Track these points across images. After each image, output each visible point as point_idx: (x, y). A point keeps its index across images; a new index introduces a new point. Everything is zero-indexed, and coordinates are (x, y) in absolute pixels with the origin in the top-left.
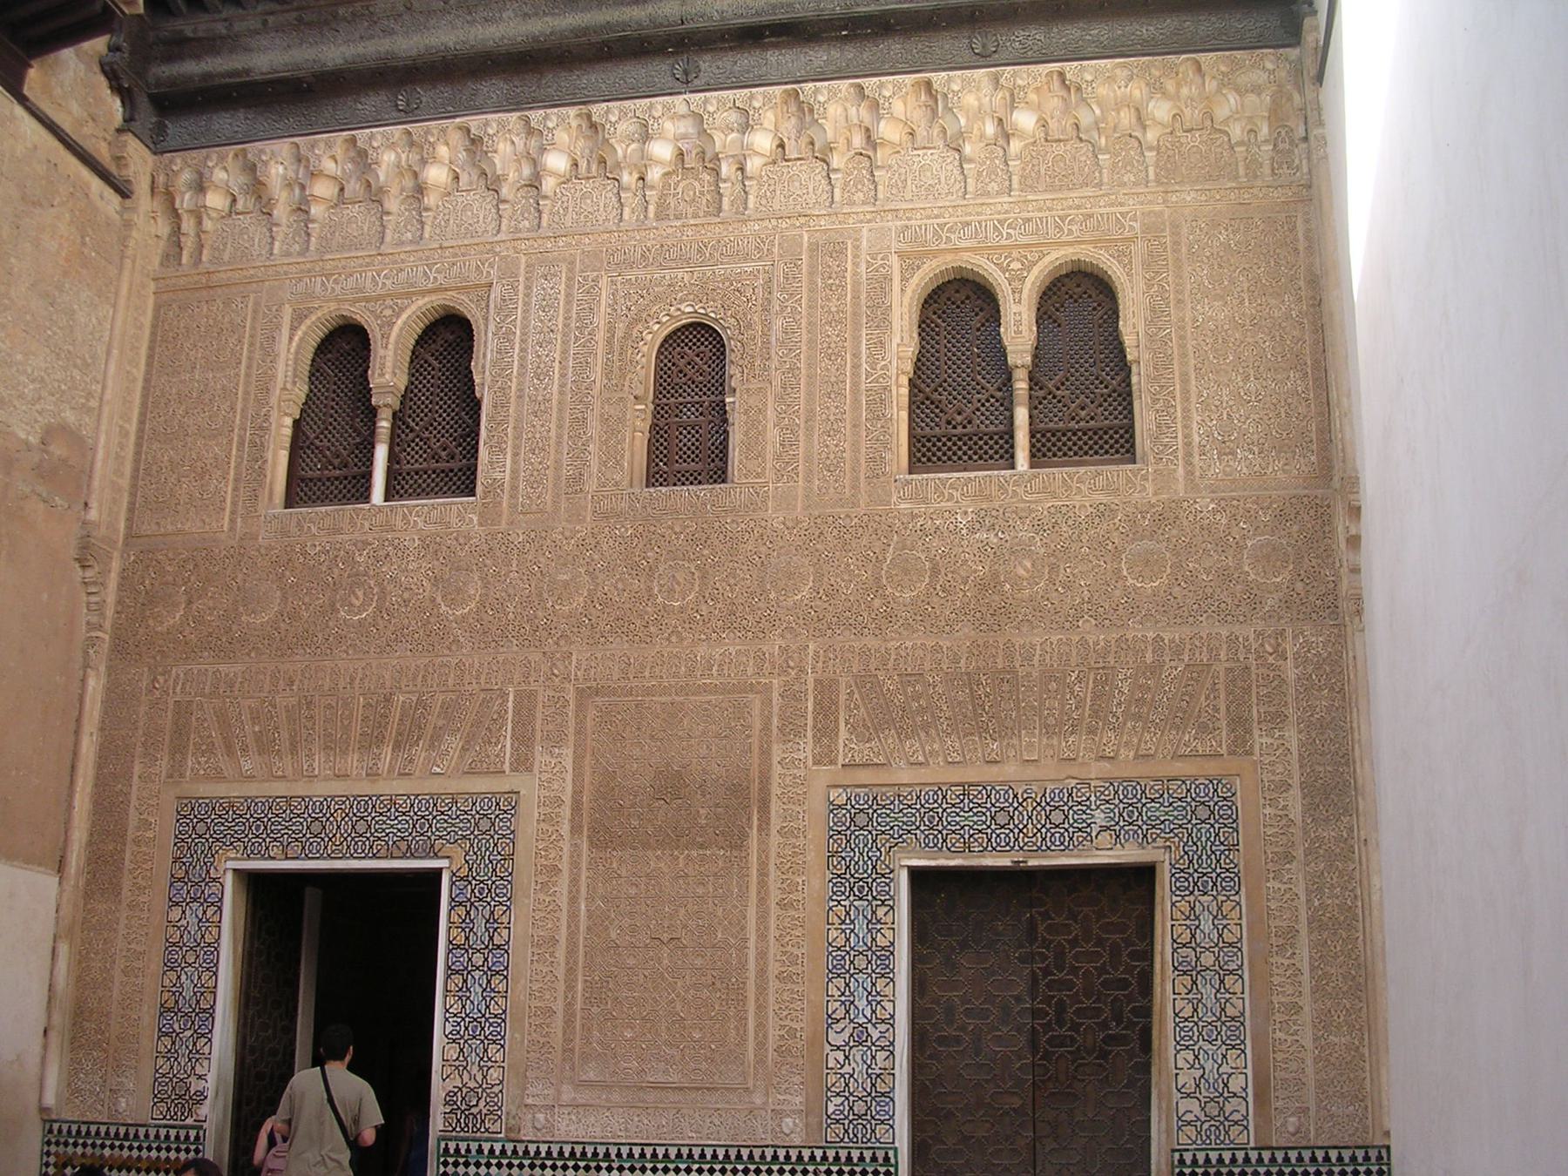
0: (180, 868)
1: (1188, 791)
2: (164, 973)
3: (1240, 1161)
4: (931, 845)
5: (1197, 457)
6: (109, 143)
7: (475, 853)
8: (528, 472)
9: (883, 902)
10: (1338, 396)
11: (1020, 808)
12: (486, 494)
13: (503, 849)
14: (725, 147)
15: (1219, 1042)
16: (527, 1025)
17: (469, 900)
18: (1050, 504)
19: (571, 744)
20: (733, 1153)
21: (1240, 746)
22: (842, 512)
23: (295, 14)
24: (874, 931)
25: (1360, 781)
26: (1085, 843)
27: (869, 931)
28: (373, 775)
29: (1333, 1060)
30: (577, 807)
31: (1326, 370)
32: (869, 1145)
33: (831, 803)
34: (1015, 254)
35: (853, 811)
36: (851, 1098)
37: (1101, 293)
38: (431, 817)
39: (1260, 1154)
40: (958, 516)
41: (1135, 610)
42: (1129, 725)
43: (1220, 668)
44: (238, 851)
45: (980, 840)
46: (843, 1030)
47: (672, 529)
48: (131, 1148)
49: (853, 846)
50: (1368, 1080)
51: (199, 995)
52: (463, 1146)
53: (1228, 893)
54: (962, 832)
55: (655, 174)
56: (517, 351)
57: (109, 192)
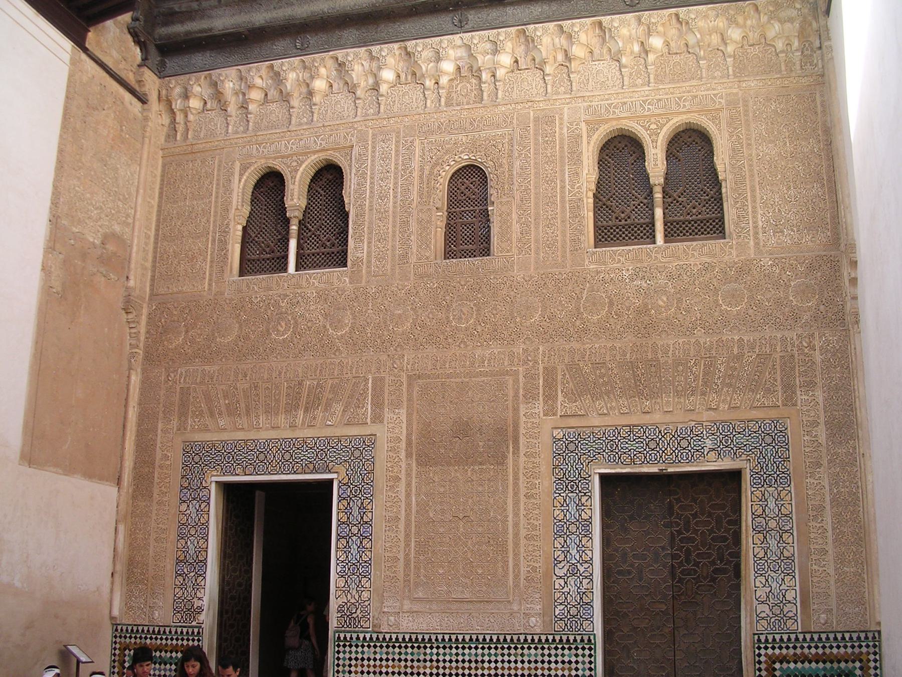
0: (186, 481)
1: (760, 427)
2: (178, 540)
3: (793, 640)
4: (612, 460)
5: (761, 235)
6: (134, 73)
7: (352, 470)
8: (377, 253)
9: (585, 494)
10: (842, 197)
11: (663, 439)
12: (353, 265)
13: (368, 467)
14: (484, 63)
15: (780, 572)
16: (383, 567)
17: (349, 496)
18: (677, 264)
19: (405, 406)
20: (502, 638)
21: (789, 401)
24: (580, 510)
25: (859, 420)
26: (700, 458)
27: (577, 510)
28: (293, 426)
29: (846, 581)
30: (409, 443)
31: (835, 182)
32: (579, 632)
33: (554, 438)
34: (653, 120)
35: (567, 442)
36: (569, 606)
37: (703, 141)
38: (326, 450)
39: (804, 636)
40: (624, 272)
41: (727, 323)
43: (777, 356)
44: (218, 471)
45: (640, 458)
46: (563, 567)
47: (459, 283)
48: (161, 639)
49: (567, 462)
50: (867, 592)
51: (198, 553)
52: (348, 636)
53: (784, 486)
54: (629, 453)
55: (444, 80)
56: (368, 184)
57: (135, 101)
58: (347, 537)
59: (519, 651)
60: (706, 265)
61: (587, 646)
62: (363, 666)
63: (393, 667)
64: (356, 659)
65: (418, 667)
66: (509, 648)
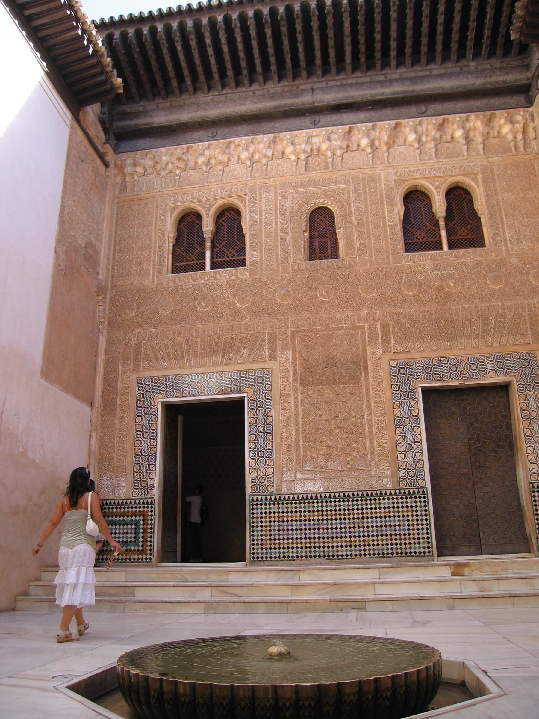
12: (251, 265)
20: (365, 493)
22: (384, 266)
23: (169, 104)
27: (409, 410)
30: (295, 373)
42: (496, 334)
43: (526, 314)
48: (124, 508)
52: (259, 498)
57: (102, 164)
58: (256, 434)
59: (377, 501)
60: (477, 262)
61: (422, 496)
62: (270, 517)
63: (292, 517)
64: (266, 513)
65: (309, 516)
66: (370, 500)
